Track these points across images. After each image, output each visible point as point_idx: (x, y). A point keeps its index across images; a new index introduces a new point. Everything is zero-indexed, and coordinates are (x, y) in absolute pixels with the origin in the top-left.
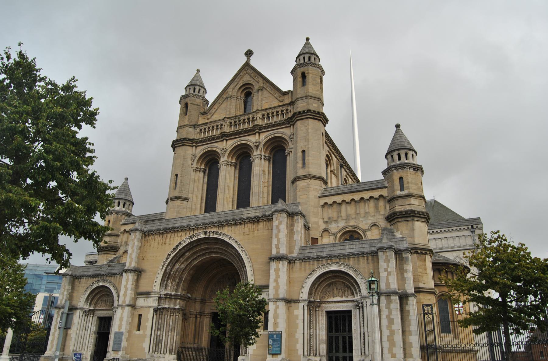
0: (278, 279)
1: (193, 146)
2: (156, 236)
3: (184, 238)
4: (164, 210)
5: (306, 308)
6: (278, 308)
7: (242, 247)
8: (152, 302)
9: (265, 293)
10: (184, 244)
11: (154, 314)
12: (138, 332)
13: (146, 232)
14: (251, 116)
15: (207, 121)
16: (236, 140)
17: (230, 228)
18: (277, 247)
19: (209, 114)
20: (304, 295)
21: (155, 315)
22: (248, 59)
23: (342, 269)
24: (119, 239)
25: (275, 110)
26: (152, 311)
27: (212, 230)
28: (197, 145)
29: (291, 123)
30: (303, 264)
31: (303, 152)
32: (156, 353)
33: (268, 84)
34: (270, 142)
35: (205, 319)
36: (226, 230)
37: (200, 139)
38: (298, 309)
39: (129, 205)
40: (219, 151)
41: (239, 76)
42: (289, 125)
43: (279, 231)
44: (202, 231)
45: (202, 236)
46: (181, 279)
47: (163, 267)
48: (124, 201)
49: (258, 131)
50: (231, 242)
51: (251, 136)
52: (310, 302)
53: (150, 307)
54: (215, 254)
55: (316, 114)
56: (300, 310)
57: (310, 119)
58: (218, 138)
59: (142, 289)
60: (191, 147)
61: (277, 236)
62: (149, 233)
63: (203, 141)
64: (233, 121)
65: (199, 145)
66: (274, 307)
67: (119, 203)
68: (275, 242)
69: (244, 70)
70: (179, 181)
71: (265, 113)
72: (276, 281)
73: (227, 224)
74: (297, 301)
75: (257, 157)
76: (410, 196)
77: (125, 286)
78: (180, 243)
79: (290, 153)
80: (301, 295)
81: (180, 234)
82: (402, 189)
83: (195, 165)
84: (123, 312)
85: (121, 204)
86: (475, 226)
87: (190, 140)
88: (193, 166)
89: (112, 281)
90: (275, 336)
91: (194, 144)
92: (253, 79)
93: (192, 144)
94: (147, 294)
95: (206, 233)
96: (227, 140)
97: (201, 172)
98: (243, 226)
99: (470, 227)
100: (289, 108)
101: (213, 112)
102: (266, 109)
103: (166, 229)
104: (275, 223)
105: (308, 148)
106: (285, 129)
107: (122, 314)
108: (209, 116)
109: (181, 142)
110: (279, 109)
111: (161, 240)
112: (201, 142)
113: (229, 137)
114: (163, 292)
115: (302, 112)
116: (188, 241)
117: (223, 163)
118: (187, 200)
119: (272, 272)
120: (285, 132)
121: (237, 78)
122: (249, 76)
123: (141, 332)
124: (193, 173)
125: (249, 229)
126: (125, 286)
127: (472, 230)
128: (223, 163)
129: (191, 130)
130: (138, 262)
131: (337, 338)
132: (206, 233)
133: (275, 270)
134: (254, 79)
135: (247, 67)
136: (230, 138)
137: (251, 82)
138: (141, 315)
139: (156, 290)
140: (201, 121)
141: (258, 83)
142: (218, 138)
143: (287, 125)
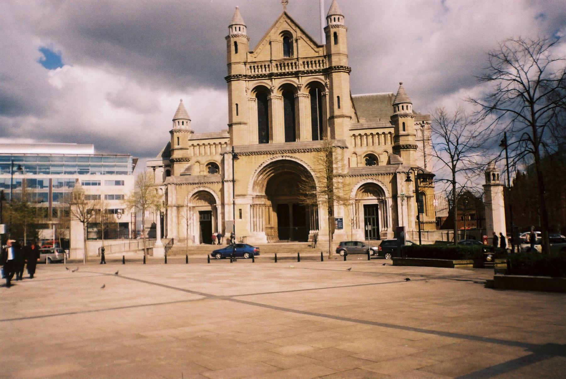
1: (246, 81)
3: (266, 159)
8: (249, 201)
12: (241, 220)
14: (293, 61)
15: (254, 60)
23: (375, 182)
25: (313, 60)
31: (338, 97)
32: (255, 232)
36: (297, 155)
39: (187, 122)
45: (281, 158)
46: (263, 186)
47: (252, 178)
57: (342, 72)
64: (278, 64)
76: (408, 135)
78: (264, 162)
81: (263, 156)
82: (404, 130)
86: (425, 122)
87: (244, 76)
90: (339, 219)
95: (282, 157)
99: (421, 122)
102: (306, 58)
110: (317, 59)
114: (255, 194)
116: (269, 162)
127: (423, 125)
128: (274, 97)
131: (369, 219)
134: (292, 28)
140: (251, 58)
141: (296, 32)
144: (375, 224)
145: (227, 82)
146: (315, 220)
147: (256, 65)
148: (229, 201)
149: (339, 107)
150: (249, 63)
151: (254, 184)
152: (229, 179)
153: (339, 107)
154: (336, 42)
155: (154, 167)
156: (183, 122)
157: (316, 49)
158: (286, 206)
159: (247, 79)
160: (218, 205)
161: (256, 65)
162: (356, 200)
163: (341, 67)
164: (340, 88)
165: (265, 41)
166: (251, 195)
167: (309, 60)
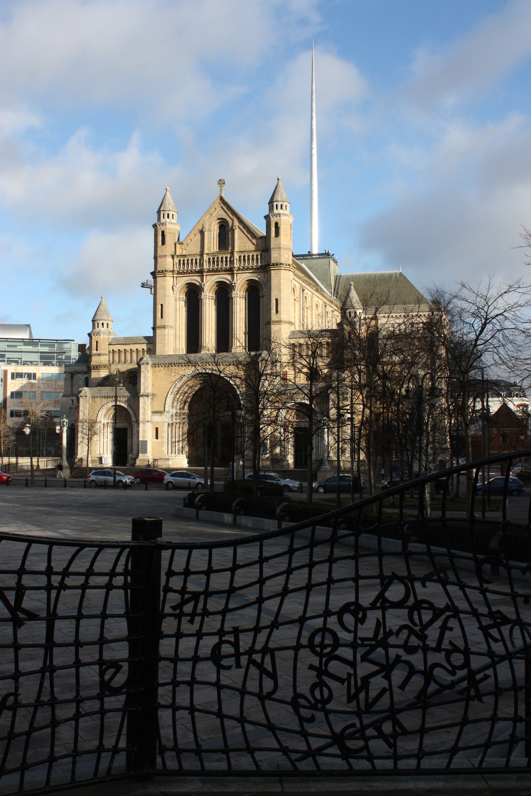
26: (166, 425)
32: (173, 455)
67: (103, 324)
77: (143, 407)
81: (184, 368)
100: (263, 254)
102: (243, 252)
105: (280, 297)
107: (144, 428)
123: (159, 440)
148: (144, 418)
149: (277, 311)
150: (178, 256)
151: (174, 400)
153: (277, 311)
154: (277, 234)
155: (72, 373)
164: (280, 290)
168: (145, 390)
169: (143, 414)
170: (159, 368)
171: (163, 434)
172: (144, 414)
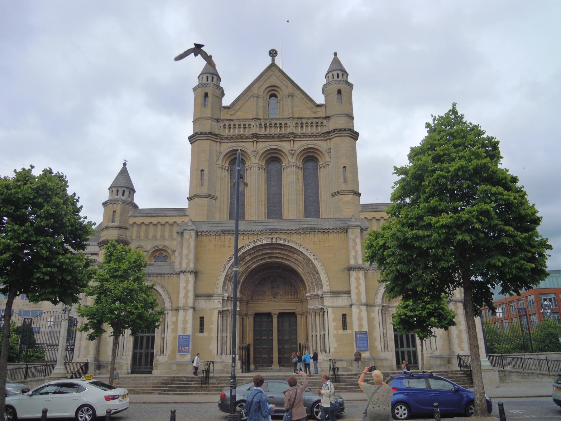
0: (360, 287)
1: (217, 142)
2: (212, 237)
4: (187, 207)
5: (380, 311)
6: (362, 311)
7: (314, 255)
9: (342, 298)
10: (247, 248)
11: (218, 316)
12: (201, 334)
13: (199, 232)
16: (268, 143)
17: (299, 236)
18: (355, 258)
19: (231, 110)
20: (379, 300)
21: (219, 317)
22: (273, 60)
24: (128, 233)
25: (309, 121)
26: (216, 313)
27: (280, 236)
28: (221, 141)
29: (328, 137)
30: (375, 273)
33: (299, 92)
34: (304, 152)
35: (248, 320)
36: (295, 237)
37: (227, 136)
38: (373, 312)
40: (249, 152)
41: (265, 75)
42: (325, 139)
43: (356, 244)
44: (267, 236)
45: (268, 241)
47: (224, 270)
48: (122, 189)
49: (293, 139)
50: (301, 249)
51: (284, 142)
52: (383, 306)
53: (214, 309)
54: (275, 259)
55: (354, 133)
56: (376, 312)
57: (348, 137)
58: (247, 138)
59: (201, 291)
60: (216, 143)
61: (354, 248)
62: (203, 233)
63: (230, 138)
64: (263, 123)
65: (224, 141)
66: (358, 310)
68: (353, 253)
69: (269, 71)
70: (206, 177)
71: (299, 122)
72: (357, 288)
73: (295, 232)
74: (374, 305)
75: (293, 164)
78: (243, 246)
79: (327, 166)
80: (376, 301)
83: (220, 162)
84: (186, 315)
85: (120, 193)
88: (218, 163)
89: (159, 281)
91: (219, 140)
92: (281, 82)
93: (217, 139)
94: (209, 296)
95: (272, 239)
96: (257, 142)
97: (226, 170)
98: (313, 235)
100: (325, 122)
101: (237, 108)
102: (301, 118)
103: (225, 231)
104: (351, 236)
106: (320, 141)
107: (185, 317)
108: (233, 112)
109: (206, 136)
110: (314, 121)
111: (218, 242)
112: (227, 138)
113: (260, 139)
114: (226, 295)
115: (343, 130)
116: (252, 246)
117: (254, 165)
118: (215, 198)
119: (353, 280)
120: (321, 145)
121: (263, 77)
122: (276, 78)
123: (205, 334)
124: (219, 171)
125: (320, 239)
126: (185, 288)
128: (254, 165)
129: (215, 124)
130: (195, 264)
132: (272, 239)
133: (356, 278)
135: (273, 68)
136: (260, 140)
137: (279, 85)
138: (203, 317)
139: (219, 293)
141: (287, 88)
142: (247, 138)
143: (323, 139)
144: (411, 343)
145: (191, 144)
146: (318, 336)
147: (232, 124)
148: (186, 303)
151: (226, 279)
152: (188, 269)
156: (124, 192)
157: (315, 109)
158: (269, 315)
159: (219, 140)
160: (167, 309)
161: (232, 124)
162: (383, 306)
163: (348, 131)
165: (245, 96)
166: (219, 295)
167: (304, 121)
168: (188, 264)
169: (184, 297)
170: (208, 238)
171: (211, 326)
172: (186, 297)
